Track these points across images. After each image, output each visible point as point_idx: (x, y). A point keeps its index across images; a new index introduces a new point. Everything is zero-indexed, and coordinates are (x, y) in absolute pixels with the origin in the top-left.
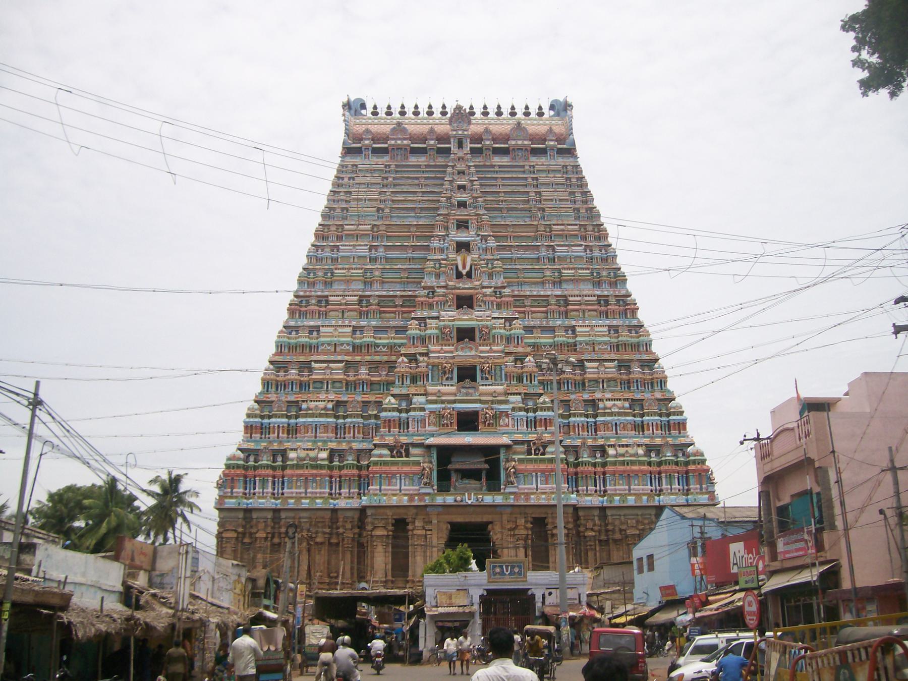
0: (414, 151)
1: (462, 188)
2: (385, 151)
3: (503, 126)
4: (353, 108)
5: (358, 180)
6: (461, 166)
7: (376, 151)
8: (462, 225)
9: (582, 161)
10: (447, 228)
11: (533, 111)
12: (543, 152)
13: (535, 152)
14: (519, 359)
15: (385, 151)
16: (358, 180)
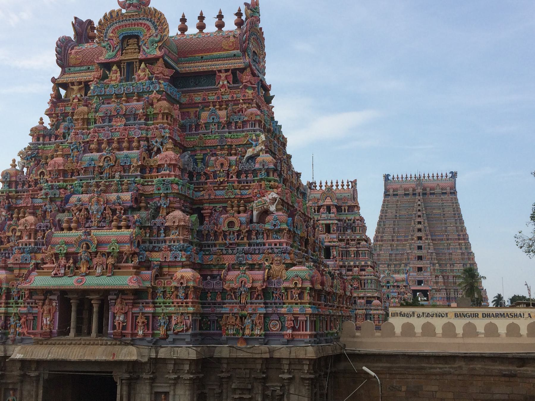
0: (405, 194)
1: (419, 210)
2: (397, 195)
3: (434, 185)
4: (386, 177)
5: (389, 206)
6: (419, 203)
7: (394, 195)
8: (419, 223)
9: (458, 197)
10: (415, 224)
11: (444, 175)
12: (446, 193)
13: (443, 193)
14: (434, 264)
15: (397, 195)
16: (389, 206)
